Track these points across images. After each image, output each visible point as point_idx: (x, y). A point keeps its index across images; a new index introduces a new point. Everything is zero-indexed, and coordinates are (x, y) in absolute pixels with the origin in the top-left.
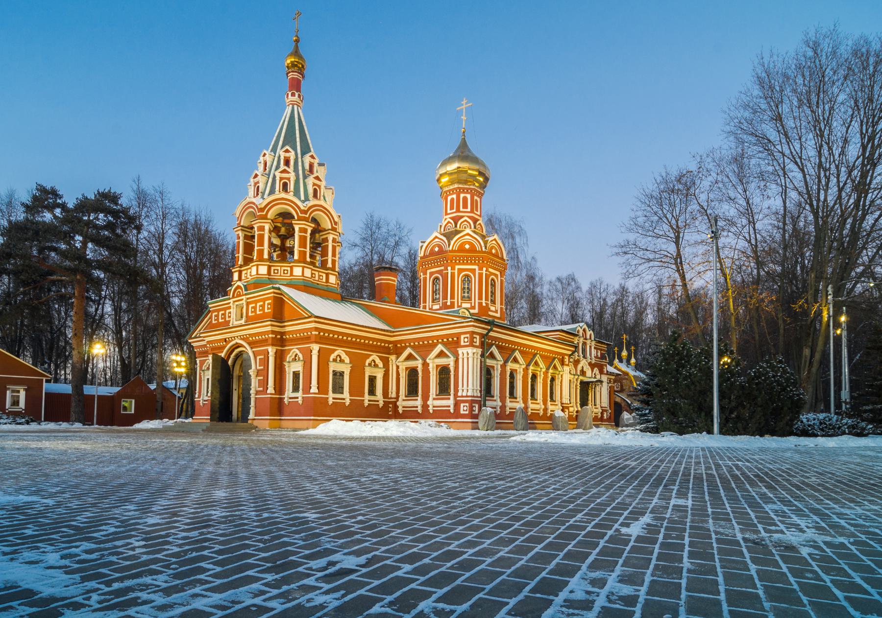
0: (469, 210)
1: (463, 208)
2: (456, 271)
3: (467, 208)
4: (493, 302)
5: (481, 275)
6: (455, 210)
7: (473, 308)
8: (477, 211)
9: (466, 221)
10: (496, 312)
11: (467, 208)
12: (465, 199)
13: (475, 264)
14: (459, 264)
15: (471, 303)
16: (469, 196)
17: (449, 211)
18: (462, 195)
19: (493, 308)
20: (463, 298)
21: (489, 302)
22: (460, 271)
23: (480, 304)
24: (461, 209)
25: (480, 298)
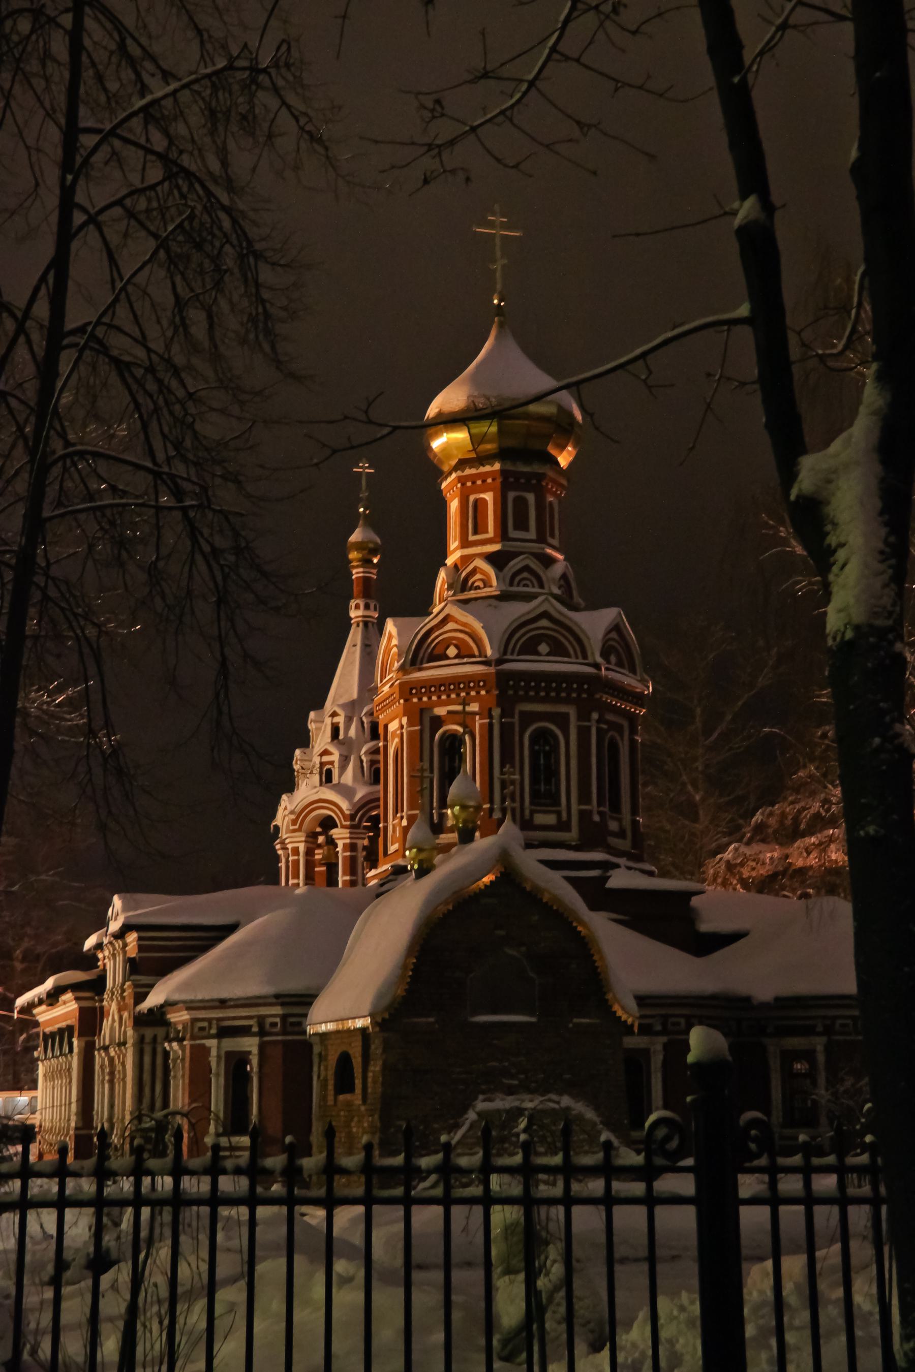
0: (532, 534)
1: (516, 528)
2: (516, 720)
3: (526, 529)
4: (615, 807)
5: (584, 733)
6: (491, 533)
7: (563, 826)
8: (553, 536)
9: (526, 568)
10: (621, 834)
11: (526, 529)
12: (521, 503)
13: (568, 701)
14: (527, 699)
15: (559, 814)
16: (531, 498)
17: (471, 538)
18: (511, 495)
19: (613, 826)
20: (535, 795)
21: (606, 809)
22: (528, 718)
23: (584, 816)
24: (513, 534)
25: (584, 797)
